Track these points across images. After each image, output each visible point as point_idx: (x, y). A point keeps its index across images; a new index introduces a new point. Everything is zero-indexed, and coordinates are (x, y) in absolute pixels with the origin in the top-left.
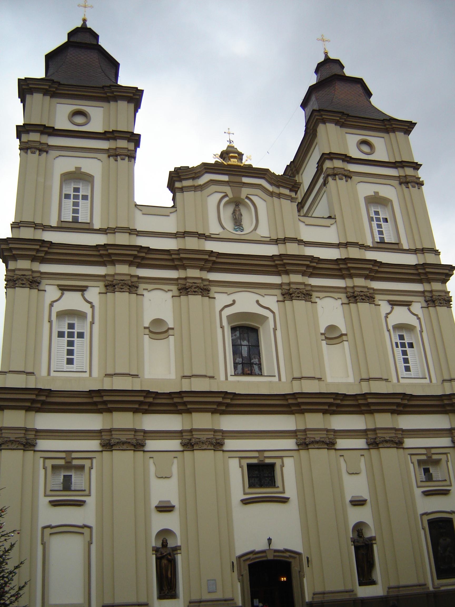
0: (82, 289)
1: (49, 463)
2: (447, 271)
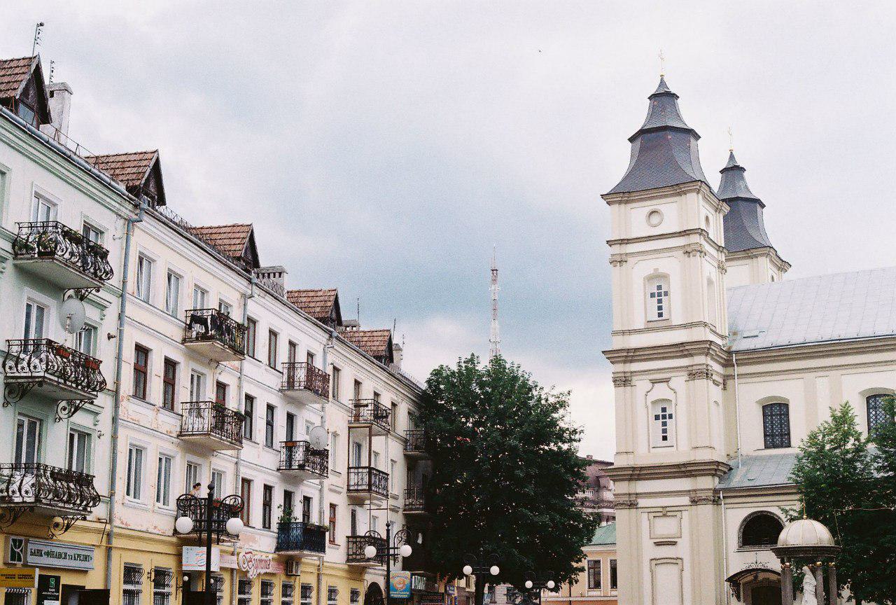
0: (667, 381)
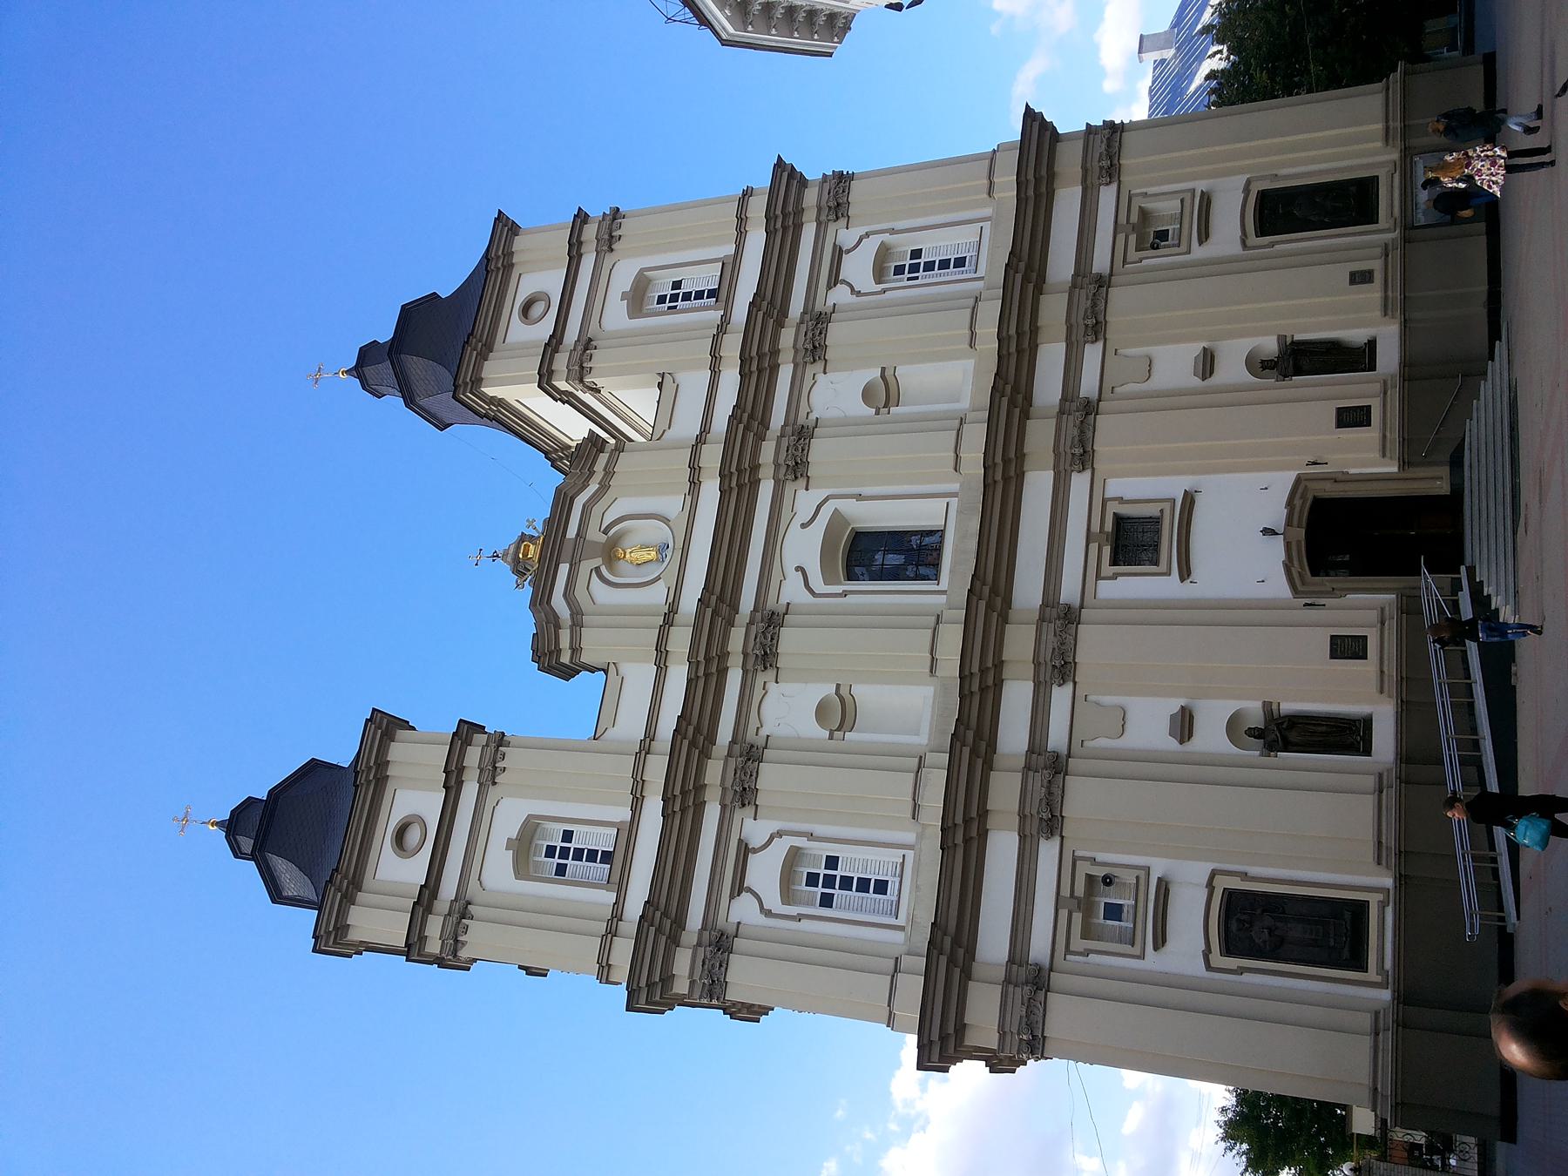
0: (745, 851)
1: (1078, 943)
2: (785, 175)
